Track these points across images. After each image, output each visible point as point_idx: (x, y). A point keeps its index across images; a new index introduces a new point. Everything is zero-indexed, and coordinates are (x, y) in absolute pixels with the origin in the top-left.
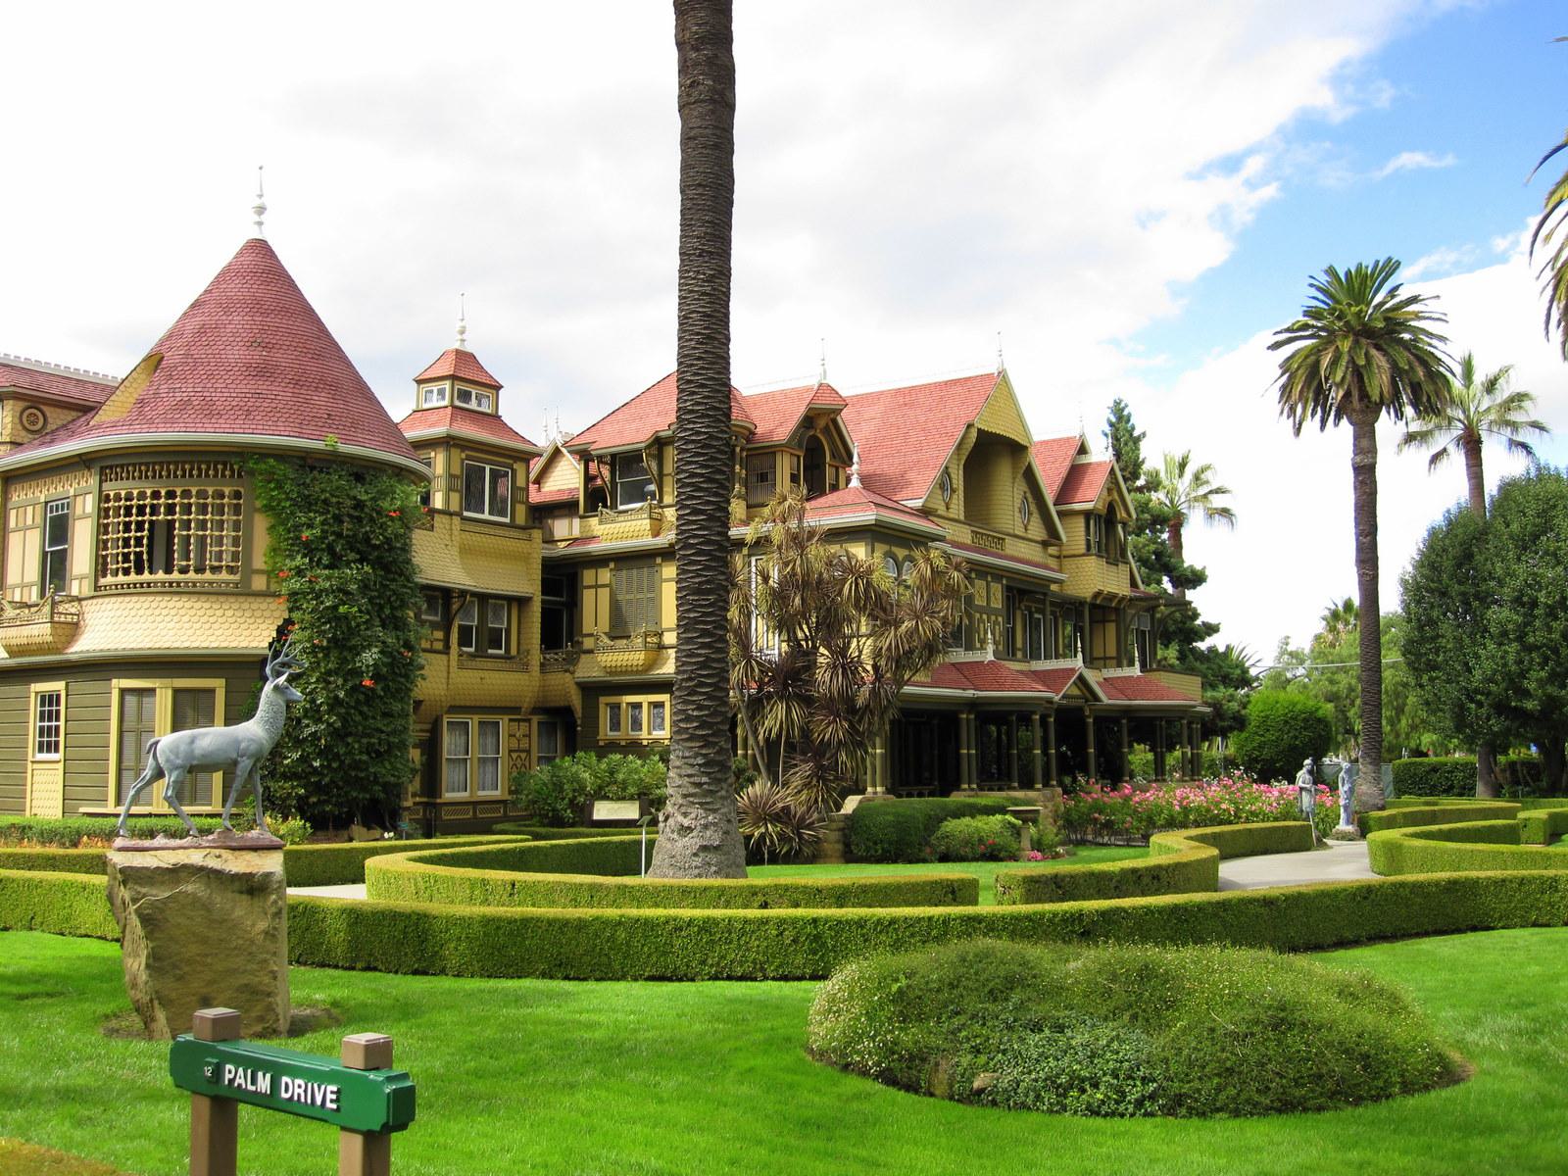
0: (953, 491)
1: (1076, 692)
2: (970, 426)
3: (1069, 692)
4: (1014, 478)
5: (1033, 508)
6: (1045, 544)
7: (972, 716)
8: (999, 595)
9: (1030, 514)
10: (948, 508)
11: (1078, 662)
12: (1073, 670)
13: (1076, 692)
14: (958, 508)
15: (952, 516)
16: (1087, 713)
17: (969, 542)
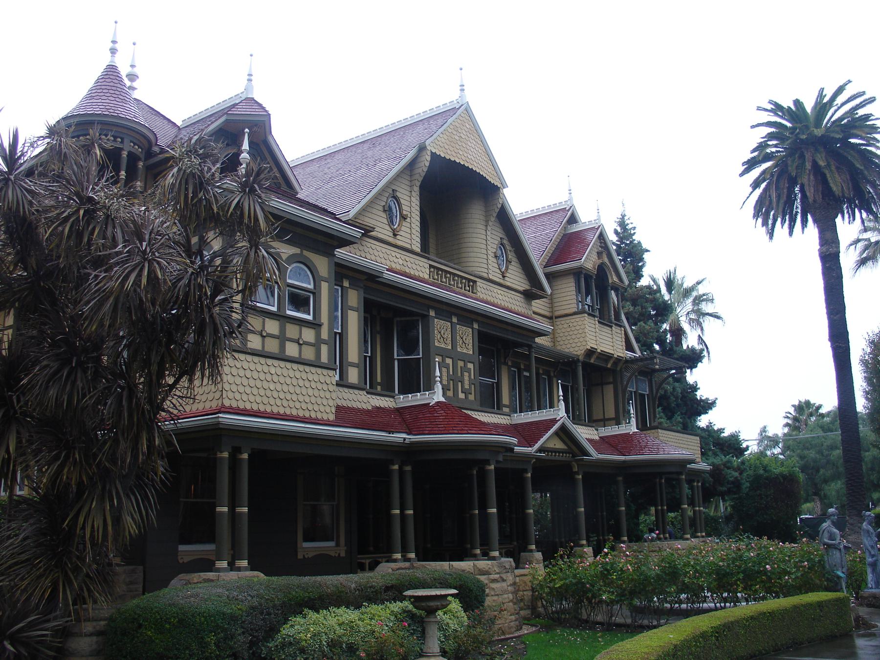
0: (404, 218)
1: (559, 445)
2: (422, 148)
3: (551, 445)
4: (487, 221)
5: (512, 256)
6: (529, 296)
7: (408, 468)
8: (469, 340)
9: (509, 262)
10: (395, 235)
11: (560, 412)
12: (554, 421)
13: (559, 445)
14: (411, 234)
15: (400, 243)
16: (576, 469)
17: (427, 277)
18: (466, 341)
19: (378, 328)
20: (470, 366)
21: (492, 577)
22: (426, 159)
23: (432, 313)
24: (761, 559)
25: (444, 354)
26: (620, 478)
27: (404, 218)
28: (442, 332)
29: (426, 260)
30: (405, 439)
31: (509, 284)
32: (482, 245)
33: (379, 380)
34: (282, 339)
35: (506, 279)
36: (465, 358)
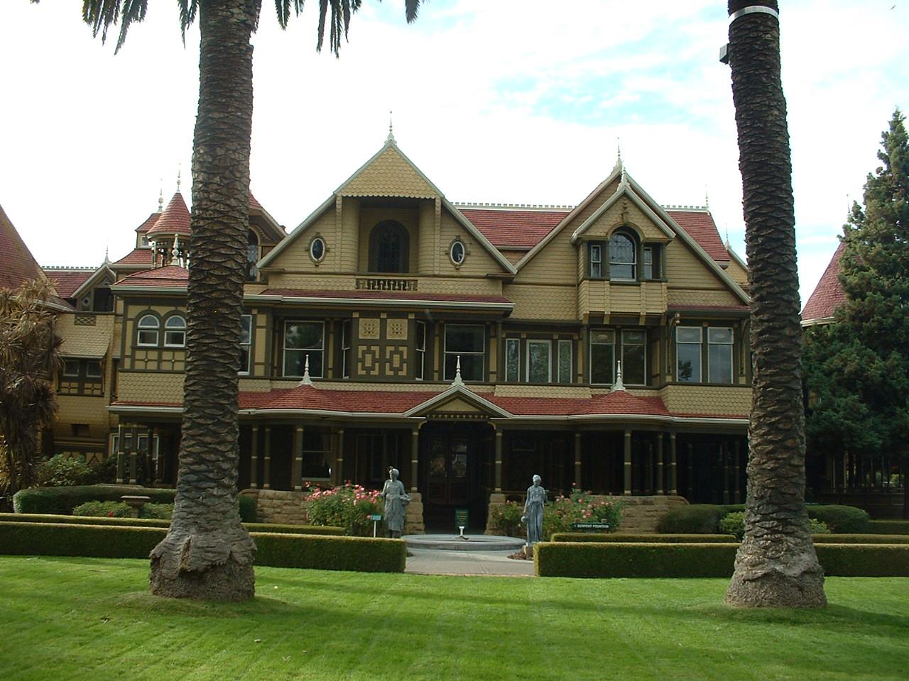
18: (399, 330)
19: (332, 330)
20: (404, 349)
21: (285, 501)
22: (339, 202)
23: (356, 315)
24: (275, 494)
25: (369, 343)
26: (577, 435)
27: (327, 251)
28: (367, 329)
29: (352, 277)
30: (249, 412)
31: (466, 274)
32: (434, 248)
33: (331, 366)
34: (160, 360)
35: (461, 270)
36: (397, 344)
